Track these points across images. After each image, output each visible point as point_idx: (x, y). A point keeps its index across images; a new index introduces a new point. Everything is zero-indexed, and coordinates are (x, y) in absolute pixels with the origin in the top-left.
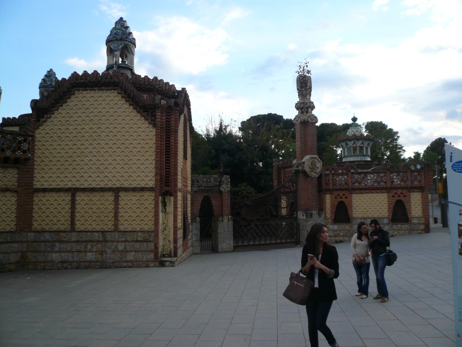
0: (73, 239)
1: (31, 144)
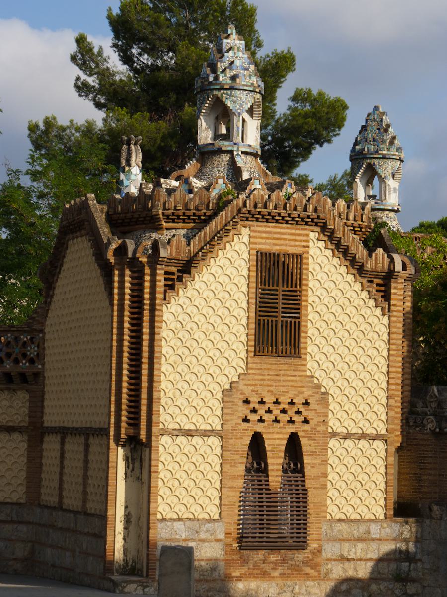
0: (60, 525)
1: (41, 345)
